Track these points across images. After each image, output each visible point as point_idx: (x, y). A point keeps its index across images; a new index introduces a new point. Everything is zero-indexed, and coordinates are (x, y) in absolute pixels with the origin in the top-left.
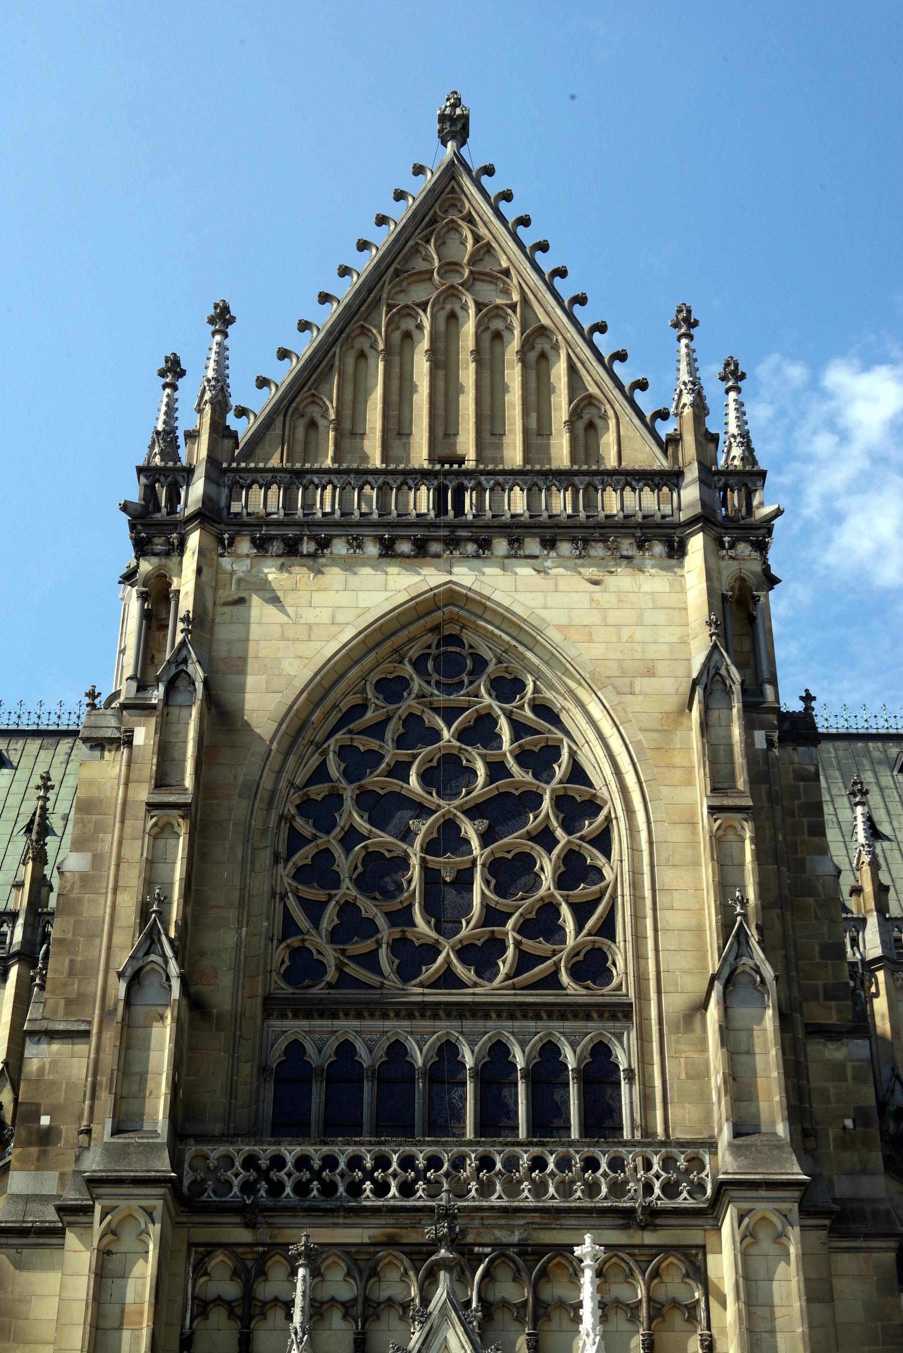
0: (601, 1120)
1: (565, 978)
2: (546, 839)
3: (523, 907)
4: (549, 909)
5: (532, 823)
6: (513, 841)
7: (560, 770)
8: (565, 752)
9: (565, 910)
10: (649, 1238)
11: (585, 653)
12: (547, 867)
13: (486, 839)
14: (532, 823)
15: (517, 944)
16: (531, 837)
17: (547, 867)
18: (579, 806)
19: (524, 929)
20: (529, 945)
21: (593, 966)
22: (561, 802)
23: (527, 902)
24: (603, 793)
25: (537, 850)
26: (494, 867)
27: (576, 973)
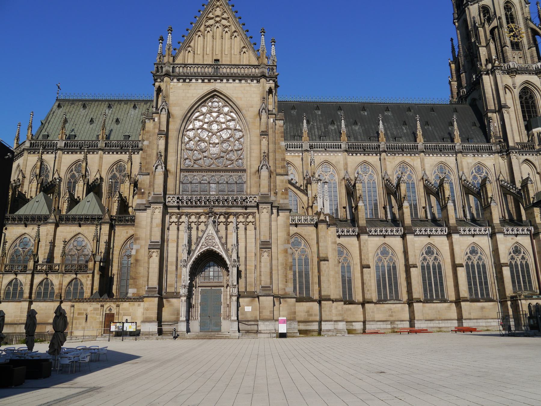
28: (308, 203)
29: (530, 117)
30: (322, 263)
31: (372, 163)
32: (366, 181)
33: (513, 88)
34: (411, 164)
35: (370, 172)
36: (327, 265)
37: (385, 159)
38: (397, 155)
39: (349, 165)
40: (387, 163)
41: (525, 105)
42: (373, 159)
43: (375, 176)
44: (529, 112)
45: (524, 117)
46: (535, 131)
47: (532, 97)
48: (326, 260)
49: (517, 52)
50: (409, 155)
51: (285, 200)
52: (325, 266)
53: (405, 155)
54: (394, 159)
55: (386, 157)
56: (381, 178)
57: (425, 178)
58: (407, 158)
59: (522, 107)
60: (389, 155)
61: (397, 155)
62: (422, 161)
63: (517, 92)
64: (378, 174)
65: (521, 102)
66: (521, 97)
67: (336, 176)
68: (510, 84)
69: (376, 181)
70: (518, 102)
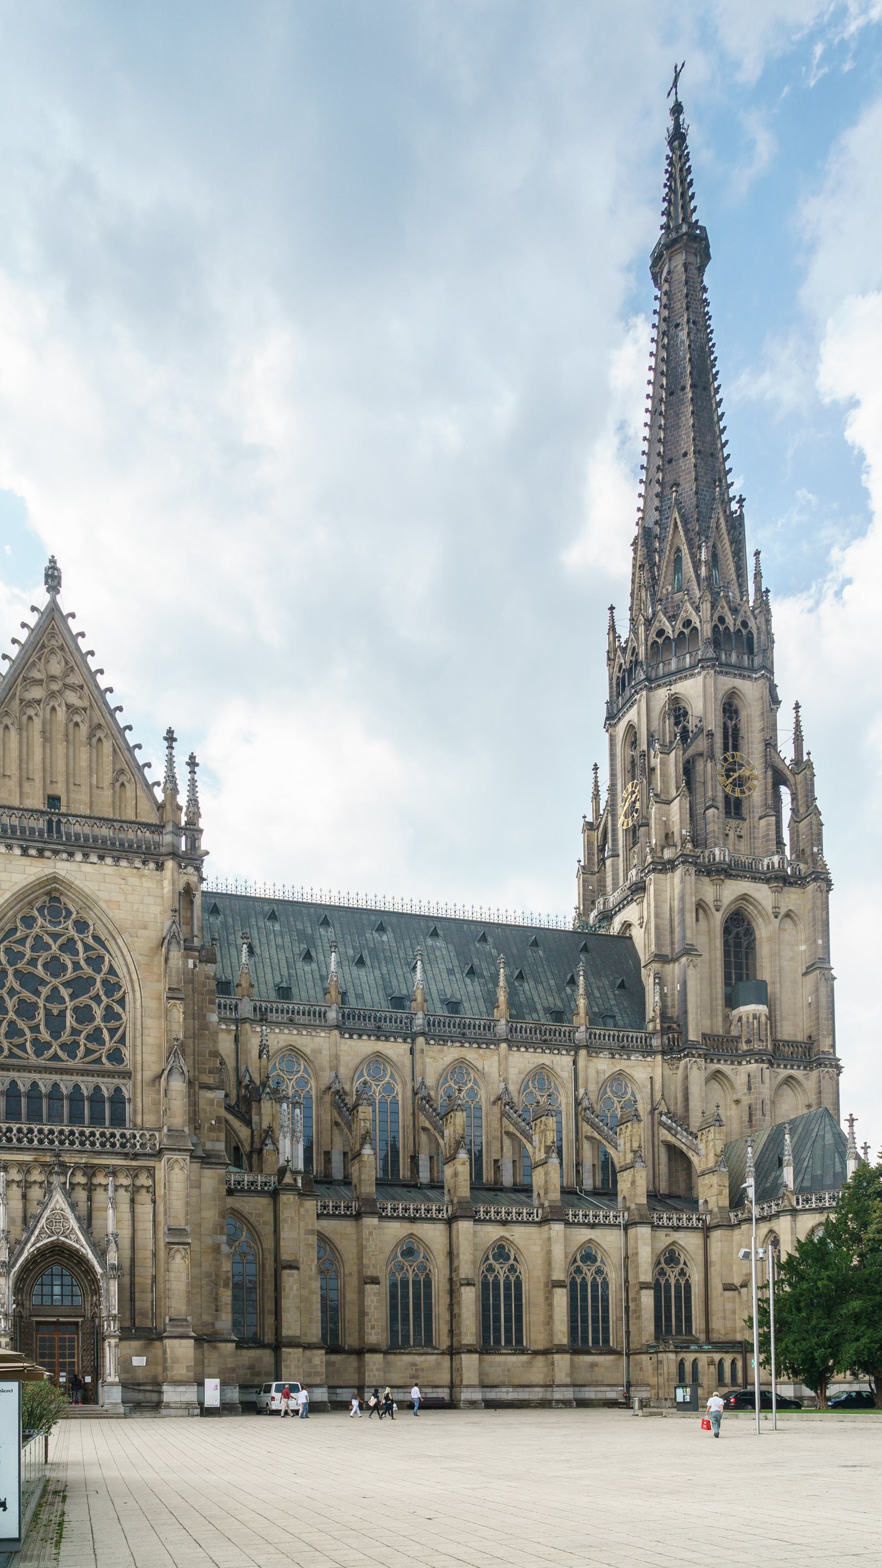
0: (118, 1120)
1: (104, 1060)
2: (97, 999)
3: (89, 1028)
4: (98, 1030)
5: (92, 993)
6: (84, 1000)
7: (105, 968)
8: (107, 959)
9: (105, 1031)
10: (134, 1163)
11: (118, 915)
12: (98, 1012)
13: (73, 996)
14: (92, 993)
15: (85, 1045)
16: (91, 998)
17: (98, 1012)
18: (111, 987)
19: (88, 1038)
20: (89, 1045)
21: (116, 1056)
22: (105, 982)
23: (89, 1027)
24: (123, 982)
25: (94, 1005)
26: (76, 1009)
27: (109, 1057)
28: (252, 1142)
29: (739, 979)
30: (286, 1272)
31: (395, 1058)
32: (378, 1097)
33: (713, 909)
34: (479, 1065)
35: (387, 1079)
36: (296, 1277)
37: (422, 1051)
38: (449, 1044)
39: (344, 1059)
40: (428, 1060)
41: (732, 949)
42: (395, 1050)
43: (398, 1088)
44: (739, 966)
45: (727, 977)
46: (747, 1010)
47: (750, 932)
48: (293, 1266)
49: (733, 823)
50: (475, 1045)
51: (217, 1143)
52: (291, 1279)
53: (467, 1045)
54: (441, 1051)
55: (425, 1047)
56: (409, 1094)
57: (506, 1099)
58: (471, 1054)
59: (727, 953)
60: (432, 1042)
61: (449, 1044)
62: (503, 1064)
63: (718, 918)
64: (404, 1084)
65: (726, 943)
66: (726, 931)
67: (313, 1083)
68: (709, 898)
69: (400, 1098)
70: (719, 942)
